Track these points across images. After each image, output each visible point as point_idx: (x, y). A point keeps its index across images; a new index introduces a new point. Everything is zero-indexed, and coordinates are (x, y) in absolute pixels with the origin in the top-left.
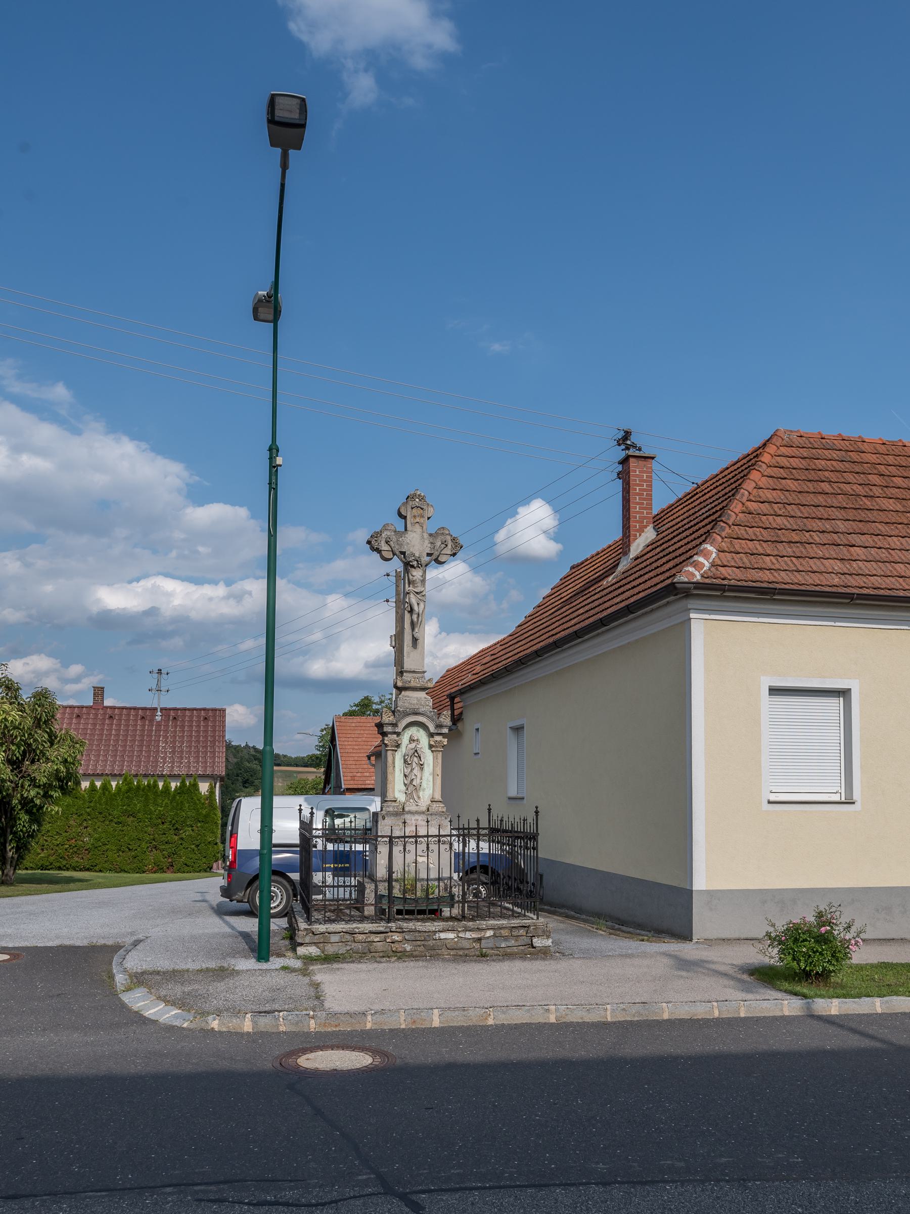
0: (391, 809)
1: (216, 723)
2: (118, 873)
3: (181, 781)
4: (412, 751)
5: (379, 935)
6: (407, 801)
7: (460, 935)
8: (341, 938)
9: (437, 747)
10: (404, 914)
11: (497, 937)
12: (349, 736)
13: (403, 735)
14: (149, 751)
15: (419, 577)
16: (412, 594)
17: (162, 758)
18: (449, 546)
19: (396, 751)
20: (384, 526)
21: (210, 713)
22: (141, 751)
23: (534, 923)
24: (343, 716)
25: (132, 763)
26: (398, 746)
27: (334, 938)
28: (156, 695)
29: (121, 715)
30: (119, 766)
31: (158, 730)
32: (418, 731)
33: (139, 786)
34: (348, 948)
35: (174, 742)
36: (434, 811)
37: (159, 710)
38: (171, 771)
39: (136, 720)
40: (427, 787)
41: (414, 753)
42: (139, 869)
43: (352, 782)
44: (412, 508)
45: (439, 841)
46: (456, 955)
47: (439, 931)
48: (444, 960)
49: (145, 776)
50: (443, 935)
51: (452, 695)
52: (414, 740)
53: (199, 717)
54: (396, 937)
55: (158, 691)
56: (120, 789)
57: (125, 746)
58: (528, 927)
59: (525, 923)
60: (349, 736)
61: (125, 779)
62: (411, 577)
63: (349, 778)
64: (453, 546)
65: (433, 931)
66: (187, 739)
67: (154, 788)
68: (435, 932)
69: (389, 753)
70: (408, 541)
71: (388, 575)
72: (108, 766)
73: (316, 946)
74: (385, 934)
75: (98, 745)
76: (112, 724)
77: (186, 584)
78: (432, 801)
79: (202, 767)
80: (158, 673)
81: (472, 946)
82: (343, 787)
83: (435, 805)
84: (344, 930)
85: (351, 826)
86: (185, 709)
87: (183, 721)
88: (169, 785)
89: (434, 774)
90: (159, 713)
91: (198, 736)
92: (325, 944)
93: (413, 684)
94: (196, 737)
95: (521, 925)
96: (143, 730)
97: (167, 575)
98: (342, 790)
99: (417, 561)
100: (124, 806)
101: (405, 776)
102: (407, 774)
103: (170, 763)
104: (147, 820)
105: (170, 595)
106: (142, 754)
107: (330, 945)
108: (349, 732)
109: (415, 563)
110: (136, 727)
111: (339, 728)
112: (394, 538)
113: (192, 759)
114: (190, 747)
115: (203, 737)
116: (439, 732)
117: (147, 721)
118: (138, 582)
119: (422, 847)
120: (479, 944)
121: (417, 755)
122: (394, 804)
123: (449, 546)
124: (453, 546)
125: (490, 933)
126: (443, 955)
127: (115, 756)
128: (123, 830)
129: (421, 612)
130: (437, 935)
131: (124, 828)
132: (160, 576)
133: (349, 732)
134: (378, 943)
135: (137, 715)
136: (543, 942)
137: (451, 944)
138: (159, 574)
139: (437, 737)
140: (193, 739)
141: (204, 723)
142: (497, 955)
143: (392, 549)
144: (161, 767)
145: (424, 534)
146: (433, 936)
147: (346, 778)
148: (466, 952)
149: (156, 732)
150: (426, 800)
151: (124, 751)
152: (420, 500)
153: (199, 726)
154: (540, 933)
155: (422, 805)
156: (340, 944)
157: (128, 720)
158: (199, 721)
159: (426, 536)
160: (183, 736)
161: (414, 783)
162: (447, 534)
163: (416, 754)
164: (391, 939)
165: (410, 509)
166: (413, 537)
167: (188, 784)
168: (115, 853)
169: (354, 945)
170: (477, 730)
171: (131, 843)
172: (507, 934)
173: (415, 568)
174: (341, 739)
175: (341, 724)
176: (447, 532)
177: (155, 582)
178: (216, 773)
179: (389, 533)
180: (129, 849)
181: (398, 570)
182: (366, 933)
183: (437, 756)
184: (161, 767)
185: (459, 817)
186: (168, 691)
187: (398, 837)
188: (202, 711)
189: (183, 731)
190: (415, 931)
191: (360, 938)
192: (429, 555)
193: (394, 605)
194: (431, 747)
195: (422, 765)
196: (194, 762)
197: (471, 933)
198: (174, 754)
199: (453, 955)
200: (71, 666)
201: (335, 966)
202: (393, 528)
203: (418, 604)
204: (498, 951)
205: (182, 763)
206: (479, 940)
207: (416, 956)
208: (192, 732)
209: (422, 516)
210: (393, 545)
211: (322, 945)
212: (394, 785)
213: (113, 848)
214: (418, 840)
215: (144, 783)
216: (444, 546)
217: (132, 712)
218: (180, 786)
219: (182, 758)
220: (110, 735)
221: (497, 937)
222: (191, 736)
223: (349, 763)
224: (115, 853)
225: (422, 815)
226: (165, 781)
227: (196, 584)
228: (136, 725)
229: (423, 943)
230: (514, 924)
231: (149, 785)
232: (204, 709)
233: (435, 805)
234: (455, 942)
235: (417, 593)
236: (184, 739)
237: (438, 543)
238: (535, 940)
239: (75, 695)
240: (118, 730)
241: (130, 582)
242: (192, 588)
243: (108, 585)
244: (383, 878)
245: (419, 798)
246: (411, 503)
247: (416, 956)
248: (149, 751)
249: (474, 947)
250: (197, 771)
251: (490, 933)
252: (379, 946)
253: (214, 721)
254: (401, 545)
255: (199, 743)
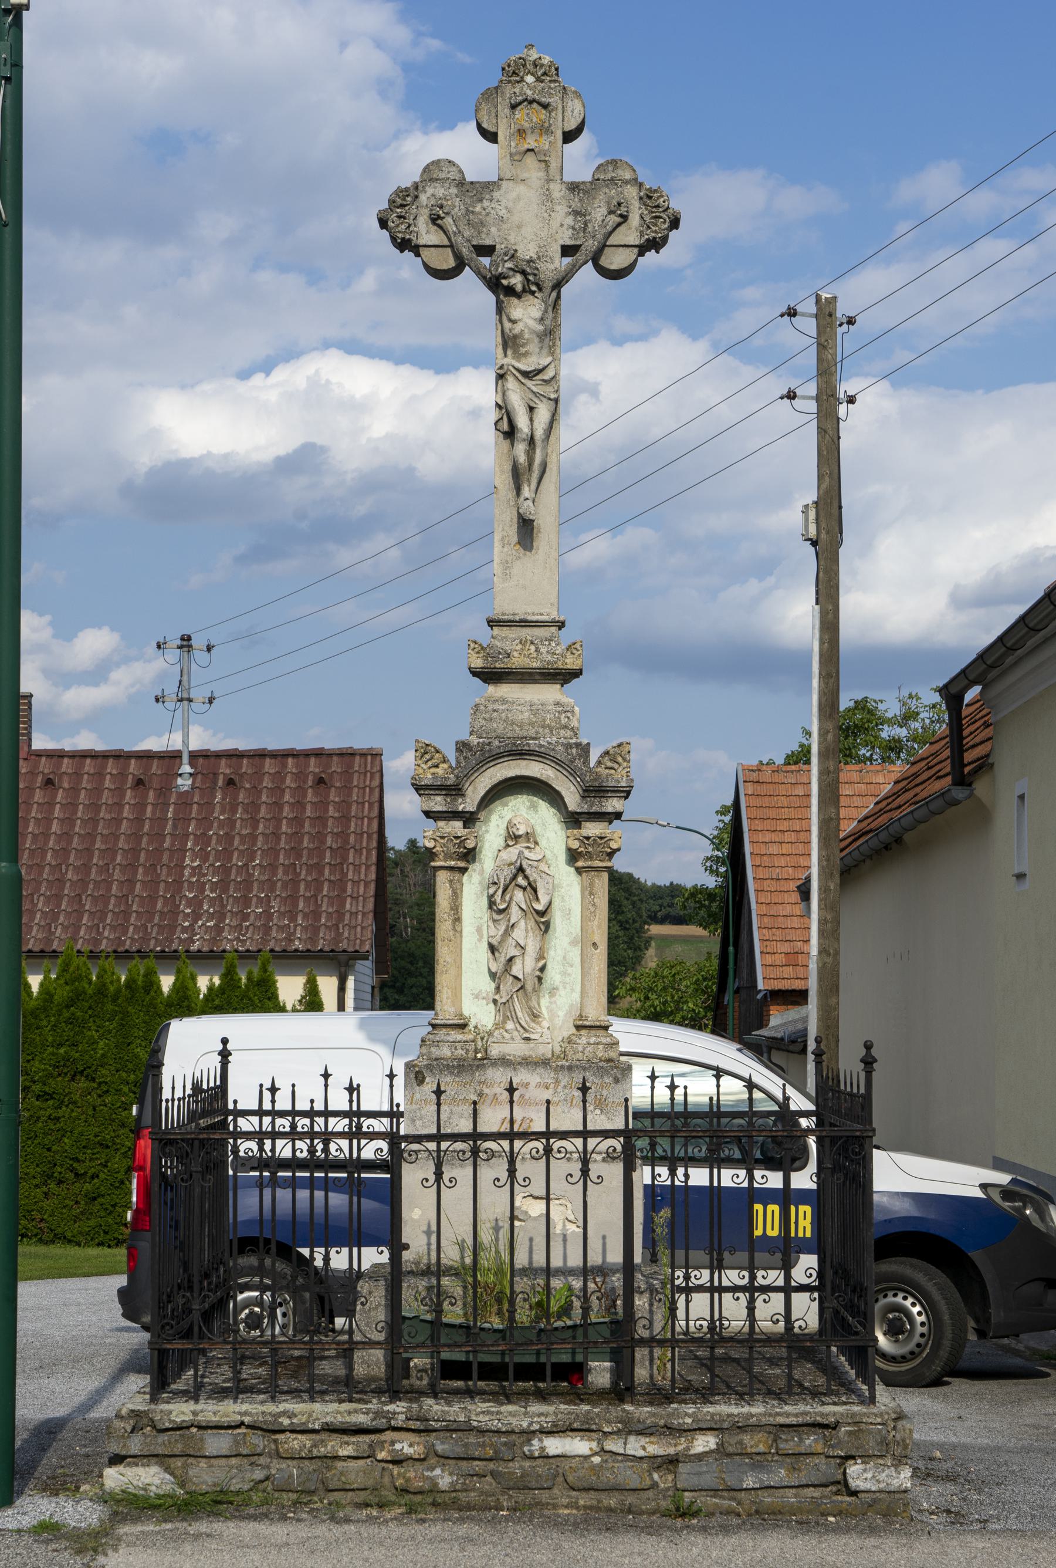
0: (446, 1052)
1: (350, 795)
2: (46, 1243)
3: (223, 971)
4: (509, 872)
5: (353, 1439)
6: (497, 1026)
7: (613, 1445)
8: (237, 1443)
9: (591, 858)
10: (475, 1375)
11: (730, 1455)
12: (784, 825)
13: (487, 821)
14: (153, 884)
15: (532, 324)
16: (510, 379)
17: (190, 902)
18: (635, 220)
19: (463, 871)
20: (427, 169)
21: (336, 765)
22: (131, 882)
23: (854, 1415)
24: (787, 763)
25: (103, 919)
26: (470, 855)
27: (217, 1443)
28: (179, 712)
29: (78, 775)
30: (65, 928)
31: (182, 820)
32: (533, 807)
33: (134, 981)
34: (259, 1474)
35: (226, 854)
36: (580, 1056)
37: (185, 758)
38: (213, 940)
39: (119, 791)
40: (564, 983)
41: (514, 877)
42: (106, 1233)
43: (788, 971)
44: (513, 107)
45: (548, 1151)
46: (597, 1509)
47: (542, 1432)
48: (560, 1524)
49: (123, 956)
50: (554, 1445)
51: (953, 690)
52: (517, 838)
53: (300, 776)
54: (407, 1446)
55: (181, 700)
56: (52, 996)
57: (86, 867)
58: (835, 1426)
59: (822, 1415)
60: (784, 825)
61: (65, 970)
62: (507, 325)
63: (780, 959)
64: (647, 219)
65: (523, 1432)
66: (265, 842)
67: (147, 992)
68: (528, 1434)
69: (442, 877)
70: (503, 212)
71: (792, 313)
72: (35, 928)
73: (161, 1464)
74: (373, 1437)
75: (104, 869)
76: (51, 804)
77: (406, 371)
78: (578, 1028)
79: (305, 929)
80: (180, 647)
81: (648, 1482)
82: (761, 986)
83: (584, 1040)
84: (247, 1420)
85: (672, 1099)
86: (261, 755)
87: (256, 790)
88: (190, 985)
89: (586, 943)
90: (186, 769)
91: (297, 836)
92: (190, 1460)
93: (518, 661)
94: (59, 837)
95: (808, 1419)
96: (139, 821)
97: (352, 347)
98: (759, 997)
99: (523, 273)
100: (61, 1045)
101: (492, 949)
102: (494, 942)
103: (211, 917)
104: (125, 1089)
105: (358, 407)
106: (132, 890)
107: (203, 1463)
108: (786, 813)
109: (517, 281)
110: (121, 812)
111: (754, 801)
112: (458, 207)
113: (276, 905)
114: (273, 867)
115: (312, 838)
116: (594, 809)
117: (151, 793)
118: (268, 374)
119: (494, 1170)
120: (670, 1477)
121: (524, 883)
122: (455, 1035)
123: (635, 220)
124: (647, 219)
125: (705, 1443)
126: (555, 1506)
127: (58, 897)
128: (58, 1119)
129: (539, 433)
130: (535, 1442)
131: (60, 1112)
132: (334, 352)
133: (786, 813)
134: (352, 1464)
135: (122, 775)
136: (882, 1476)
137: (581, 1473)
138: (326, 345)
139: (588, 825)
140: (282, 844)
141: (316, 794)
142: (729, 1512)
143: (449, 239)
144: (185, 930)
145: (552, 186)
146: (522, 1445)
147: (769, 959)
148: (631, 1499)
149: (175, 827)
150: (558, 1022)
151: (83, 883)
152: (539, 80)
153: (299, 805)
154: (871, 1446)
155: (544, 1039)
156: (234, 1461)
157: (97, 791)
158: (300, 790)
159: (557, 190)
160: (253, 837)
161: (516, 970)
162: (627, 182)
163: (520, 880)
164: (389, 1452)
165: (507, 111)
166: (518, 198)
167: (244, 980)
168: (37, 1186)
169: (276, 1466)
170: (1022, 797)
171: (81, 1157)
172: (761, 1448)
173: (519, 296)
174: (761, 837)
175: (761, 789)
176: (628, 176)
177: (317, 372)
178: (343, 945)
179: (440, 192)
180: (77, 1175)
181: (824, 295)
182: (314, 1431)
183: (591, 885)
184: (185, 930)
185: (326, 1076)
186: (210, 702)
187: (419, 1139)
188: (312, 761)
189: (255, 822)
190: (467, 1428)
191: (296, 1445)
192: (567, 251)
193: (812, 406)
194: (573, 856)
195: (541, 914)
196: (282, 915)
197: (643, 1440)
198: (225, 890)
199: (585, 1507)
200: (80, 634)
201: (202, 1526)
202: (454, 175)
203: (531, 409)
204: (734, 1499)
205: (245, 917)
206: (671, 1462)
207: (469, 1507)
208: (280, 821)
209: (545, 130)
210: (452, 228)
211: (179, 1462)
212: (459, 976)
213: (32, 1172)
214: (555, 1147)
215: (119, 980)
216: (614, 219)
217: (111, 767)
218: (220, 986)
219: (246, 901)
220: (46, 835)
221: (730, 1455)
222: (276, 835)
223: (781, 910)
224: (37, 1186)
225: (541, 1070)
226: (178, 972)
227: (438, 372)
228: (119, 805)
229: (491, 1466)
230: (788, 1415)
231: (130, 984)
232: (318, 753)
233: (584, 1040)
234: (593, 1467)
235: (526, 374)
236: (254, 844)
237: (598, 213)
238: (854, 1470)
239: (93, 719)
240: (68, 821)
241: (244, 375)
242: (423, 382)
243: (183, 387)
244: (417, 1264)
245: (535, 1016)
246: (508, 90)
247: (469, 1507)
248: (153, 884)
249: (654, 1485)
250: (290, 940)
251: (705, 1443)
252: (355, 1472)
253: (347, 789)
254: (479, 226)
255: (299, 856)
